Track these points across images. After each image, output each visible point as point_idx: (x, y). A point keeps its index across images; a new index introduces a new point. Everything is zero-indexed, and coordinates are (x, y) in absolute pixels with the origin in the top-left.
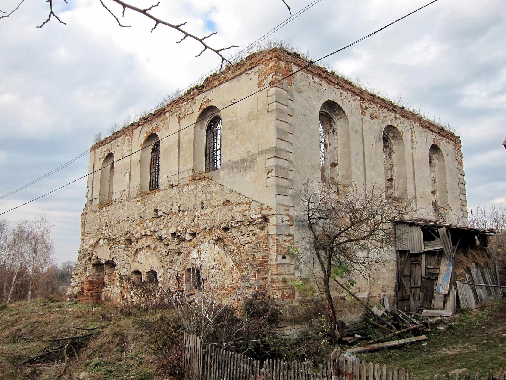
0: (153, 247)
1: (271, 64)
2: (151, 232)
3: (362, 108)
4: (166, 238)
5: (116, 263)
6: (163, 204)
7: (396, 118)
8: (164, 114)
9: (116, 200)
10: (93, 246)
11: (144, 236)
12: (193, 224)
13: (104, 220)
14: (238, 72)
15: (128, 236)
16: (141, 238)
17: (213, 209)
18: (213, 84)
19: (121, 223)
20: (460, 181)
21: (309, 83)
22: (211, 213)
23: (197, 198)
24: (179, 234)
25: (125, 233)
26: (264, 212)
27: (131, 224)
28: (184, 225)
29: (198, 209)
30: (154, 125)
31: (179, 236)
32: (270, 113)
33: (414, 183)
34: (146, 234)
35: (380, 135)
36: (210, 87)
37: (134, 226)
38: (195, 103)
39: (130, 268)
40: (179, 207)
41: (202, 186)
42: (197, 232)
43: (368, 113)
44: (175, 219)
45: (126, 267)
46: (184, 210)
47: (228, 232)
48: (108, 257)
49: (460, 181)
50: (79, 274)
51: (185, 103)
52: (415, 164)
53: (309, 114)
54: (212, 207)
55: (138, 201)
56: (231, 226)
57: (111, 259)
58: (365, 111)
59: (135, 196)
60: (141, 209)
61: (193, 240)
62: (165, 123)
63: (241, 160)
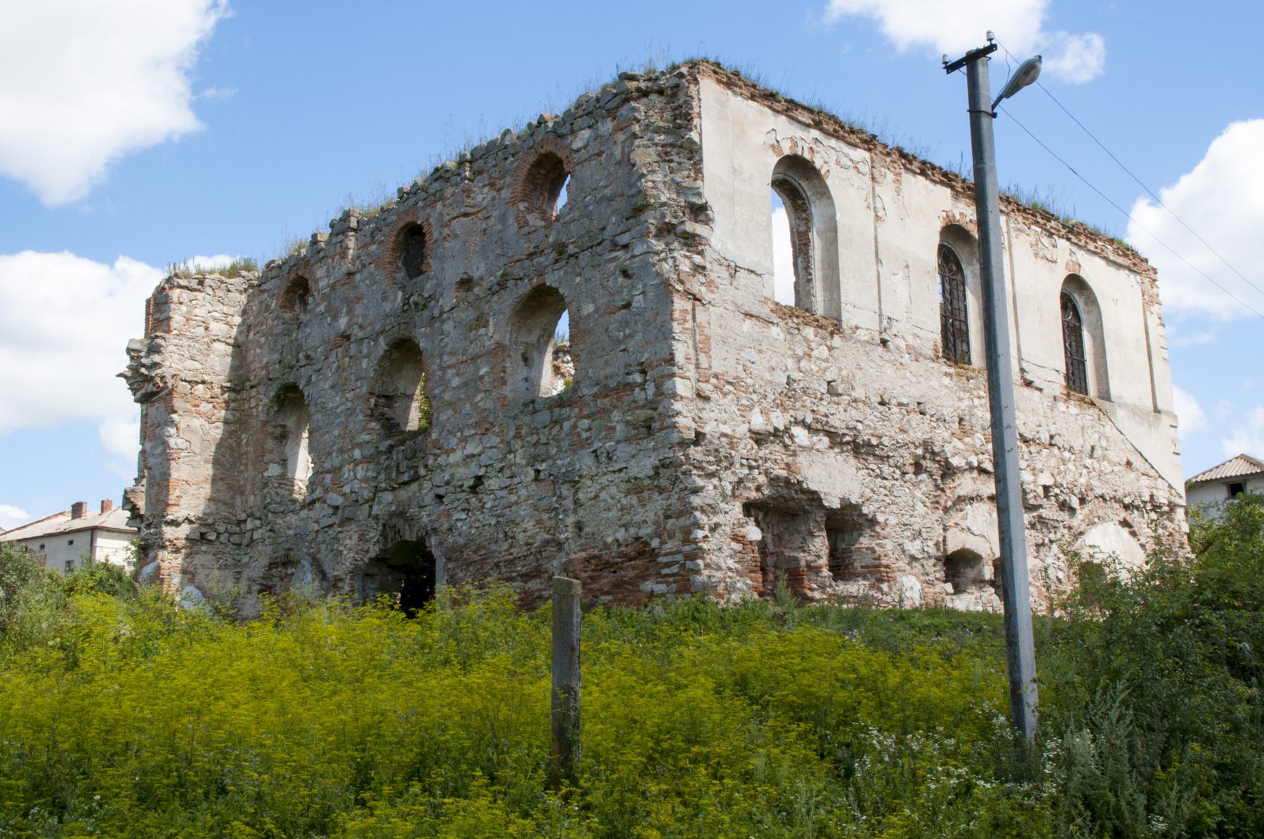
11: (971, 468)
14: (1120, 260)
24: (1057, 491)
26: (1173, 499)
28: (1069, 478)
40: (1052, 437)
55: (946, 374)
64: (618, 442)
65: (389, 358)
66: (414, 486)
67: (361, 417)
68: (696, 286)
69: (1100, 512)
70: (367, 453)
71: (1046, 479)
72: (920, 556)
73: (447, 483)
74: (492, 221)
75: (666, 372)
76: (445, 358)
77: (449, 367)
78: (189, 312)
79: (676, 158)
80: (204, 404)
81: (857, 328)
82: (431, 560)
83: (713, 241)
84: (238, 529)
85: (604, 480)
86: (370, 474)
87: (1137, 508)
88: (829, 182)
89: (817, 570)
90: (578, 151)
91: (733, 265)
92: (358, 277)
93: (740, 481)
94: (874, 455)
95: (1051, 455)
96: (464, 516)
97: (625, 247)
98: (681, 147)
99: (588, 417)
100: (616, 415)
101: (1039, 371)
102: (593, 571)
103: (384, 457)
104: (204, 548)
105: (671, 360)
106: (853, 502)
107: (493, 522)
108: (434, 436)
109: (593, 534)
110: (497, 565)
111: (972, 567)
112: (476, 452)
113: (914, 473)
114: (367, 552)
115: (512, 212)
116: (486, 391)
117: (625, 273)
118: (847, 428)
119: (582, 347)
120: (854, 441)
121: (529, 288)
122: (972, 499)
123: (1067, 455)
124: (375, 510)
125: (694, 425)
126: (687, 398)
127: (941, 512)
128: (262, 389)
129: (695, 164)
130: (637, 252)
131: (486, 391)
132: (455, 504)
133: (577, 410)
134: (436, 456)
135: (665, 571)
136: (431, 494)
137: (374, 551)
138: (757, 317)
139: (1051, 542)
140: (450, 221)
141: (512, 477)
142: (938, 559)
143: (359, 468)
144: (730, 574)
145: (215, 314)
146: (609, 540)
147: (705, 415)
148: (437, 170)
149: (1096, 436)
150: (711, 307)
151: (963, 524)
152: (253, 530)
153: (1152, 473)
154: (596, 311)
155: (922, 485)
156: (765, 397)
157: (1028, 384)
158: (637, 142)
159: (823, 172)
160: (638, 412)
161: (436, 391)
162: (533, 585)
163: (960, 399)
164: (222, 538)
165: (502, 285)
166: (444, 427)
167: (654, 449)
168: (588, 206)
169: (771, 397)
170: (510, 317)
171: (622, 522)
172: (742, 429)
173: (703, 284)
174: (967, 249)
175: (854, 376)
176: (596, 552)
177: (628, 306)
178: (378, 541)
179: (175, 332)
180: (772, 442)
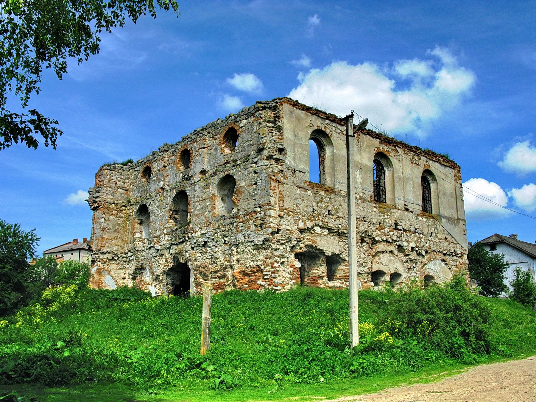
11: (383, 241)
14: (445, 164)
24: (417, 249)
26: (462, 251)
31: (417, 251)
34: (388, 240)
40: (416, 229)
55: (375, 207)
64: (251, 232)
65: (177, 197)
66: (185, 244)
67: (167, 218)
68: (280, 177)
69: (434, 257)
70: (168, 231)
71: (412, 245)
72: (362, 273)
73: (195, 243)
74: (212, 151)
75: (268, 208)
76: (195, 198)
77: (196, 202)
78: (110, 178)
79: (274, 132)
80: (114, 211)
81: (340, 191)
82: (189, 270)
83: (286, 161)
84: (125, 256)
85: (246, 245)
86: (170, 238)
87: (449, 255)
88: (331, 138)
89: (322, 277)
90: (242, 127)
91: (293, 169)
92: (167, 168)
93: (294, 246)
94: (346, 236)
95: (415, 236)
96: (200, 255)
97: (256, 163)
98: (276, 128)
99: (242, 222)
100: (251, 222)
101: (411, 205)
102: (242, 276)
103: (174, 233)
104: (113, 262)
105: (269, 204)
106: (337, 253)
107: (210, 257)
108: (191, 226)
109: (243, 263)
110: (211, 273)
111: (382, 277)
112: (205, 233)
113: (361, 243)
114: (168, 266)
115: (219, 147)
116: (209, 211)
117: (256, 172)
118: (335, 227)
119: (240, 197)
120: (338, 231)
121: (224, 175)
122: (383, 252)
123: (421, 235)
124: (171, 252)
125: (277, 226)
126: (275, 217)
127: (371, 257)
128: (134, 206)
129: (281, 134)
130: (259, 165)
131: (209, 211)
132: (198, 251)
133: (238, 220)
134: (192, 233)
135: (265, 277)
136: (190, 247)
137: (171, 265)
138: (302, 188)
139: (414, 267)
140: (198, 150)
141: (216, 242)
142: (369, 274)
143: (166, 236)
144: (287, 279)
145: (119, 179)
146: (248, 266)
147: (281, 223)
148: (195, 131)
149: (433, 229)
150: (285, 185)
151: (379, 261)
152: (130, 256)
153: (455, 242)
154: (245, 185)
155: (364, 247)
156: (304, 216)
157: (407, 210)
158: (261, 126)
159: (329, 135)
160: (258, 221)
161: (192, 210)
162: (222, 281)
163: (380, 216)
164: (120, 259)
165: (215, 174)
166: (194, 223)
167: (263, 235)
168: (244, 147)
169: (306, 216)
170: (217, 185)
171: (252, 260)
172: (296, 227)
173: (282, 176)
174: (386, 161)
175: (339, 208)
176: (243, 270)
177: (256, 183)
178: (172, 262)
179: (105, 185)
180: (306, 232)
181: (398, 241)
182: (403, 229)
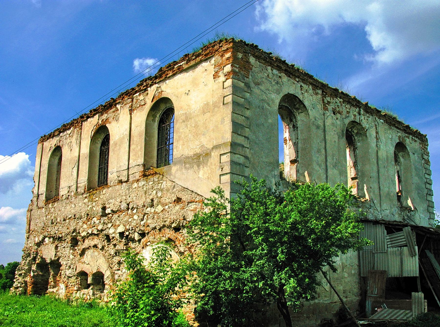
0: (100, 246)
1: (228, 55)
2: (98, 230)
3: (323, 102)
4: (113, 237)
5: (62, 263)
6: (111, 201)
7: (360, 114)
8: (116, 105)
9: (63, 196)
10: (39, 244)
12: (142, 223)
13: (50, 217)
14: (192, 63)
15: (74, 234)
16: (88, 237)
17: (164, 207)
18: (167, 74)
19: (67, 221)
20: (427, 181)
21: (268, 76)
22: (162, 211)
23: (147, 195)
24: (127, 233)
25: (72, 232)
27: (78, 221)
28: (133, 224)
29: (148, 207)
30: (105, 116)
31: (127, 236)
32: (225, 106)
33: (379, 182)
34: (93, 232)
35: (343, 131)
36: (164, 78)
37: (81, 224)
38: (148, 94)
39: (76, 269)
40: (128, 205)
41: (152, 183)
42: (147, 232)
43: (330, 108)
44: (124, 217)
45: (72, 267)
46: (133, 208)
47: (179, 232)
48: (54, 257)
49: (427, 181)
50: (23, 274)
51: (138, 94)
52: (380, 162)
53: (268, 107)
54: (164, 205)
55: (86, 197)
56: (183, 226)
57: (56, 258)
58: (327, 105)
59: (83, 191)
60: (88, 206)
61: (142, 240)
62: (116, 115)
63: (194, 155)
71: (121, 229)
181: (106, 229)
182: (112, 210)
